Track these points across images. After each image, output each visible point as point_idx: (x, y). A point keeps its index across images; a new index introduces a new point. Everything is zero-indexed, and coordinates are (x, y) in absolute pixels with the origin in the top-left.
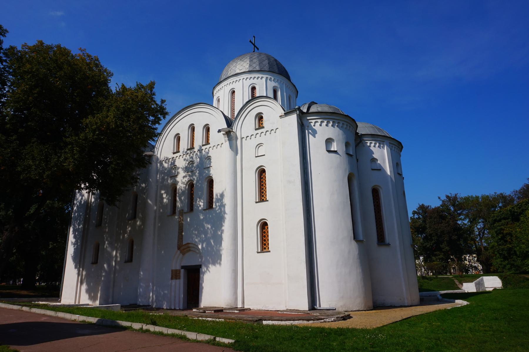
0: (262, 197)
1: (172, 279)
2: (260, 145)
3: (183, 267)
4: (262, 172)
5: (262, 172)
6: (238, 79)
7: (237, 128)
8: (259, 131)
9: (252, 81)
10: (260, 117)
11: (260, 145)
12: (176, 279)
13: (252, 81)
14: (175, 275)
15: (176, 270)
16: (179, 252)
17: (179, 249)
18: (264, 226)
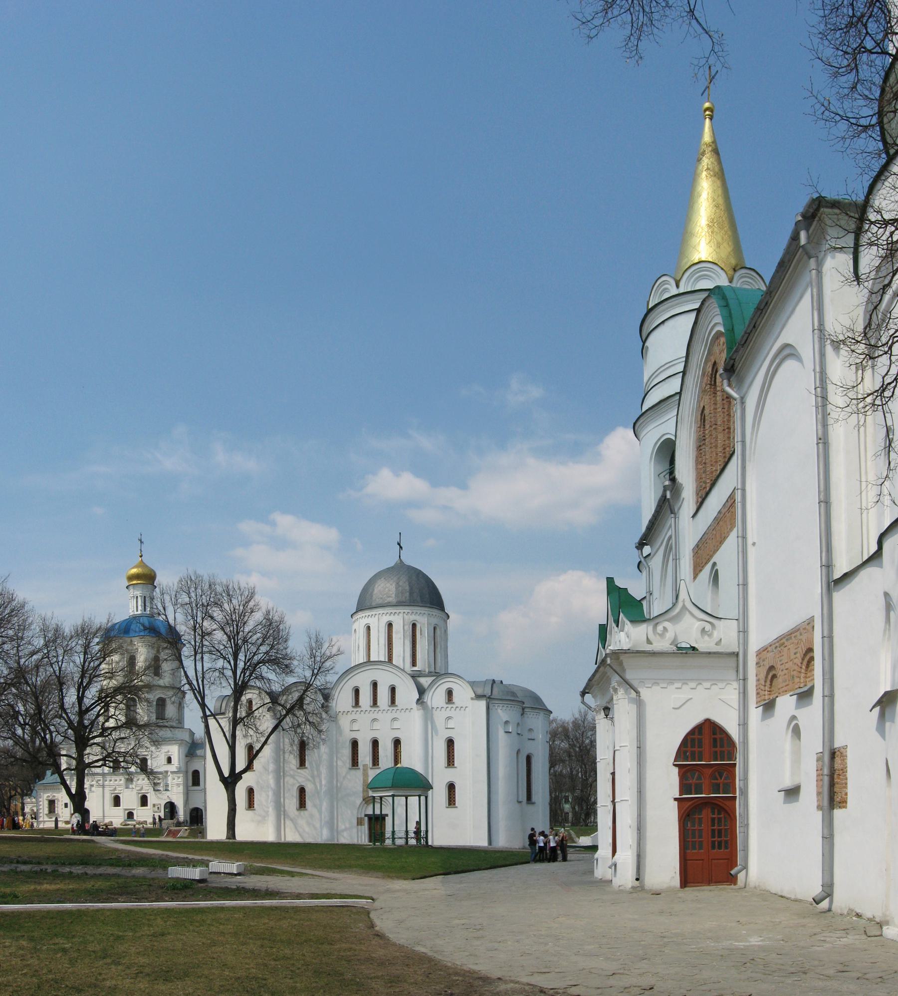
0: (450, 761)
1: (357, 825)
2: (449, 718)
3: (366, 815)
4: (450, 743)
5: (450, 743)
6: (398, 611)
7: (428, 698)
8: (450, 706)
9: (413, 618)
10: (450, 693)
11: (449, 718)
12: (361, 825)
13: (413, 618)
14: (360, 822)
15: (361, 818)
16: (364, 802)
17: (363, 800)
18: (451, 787)
